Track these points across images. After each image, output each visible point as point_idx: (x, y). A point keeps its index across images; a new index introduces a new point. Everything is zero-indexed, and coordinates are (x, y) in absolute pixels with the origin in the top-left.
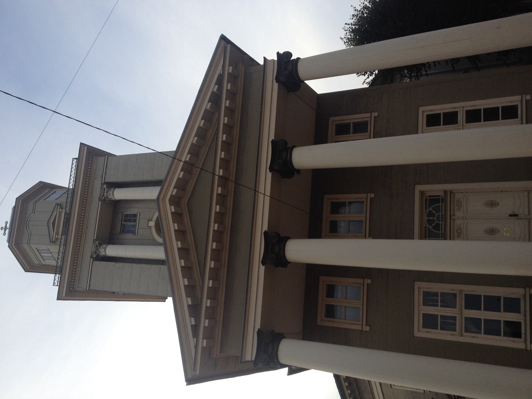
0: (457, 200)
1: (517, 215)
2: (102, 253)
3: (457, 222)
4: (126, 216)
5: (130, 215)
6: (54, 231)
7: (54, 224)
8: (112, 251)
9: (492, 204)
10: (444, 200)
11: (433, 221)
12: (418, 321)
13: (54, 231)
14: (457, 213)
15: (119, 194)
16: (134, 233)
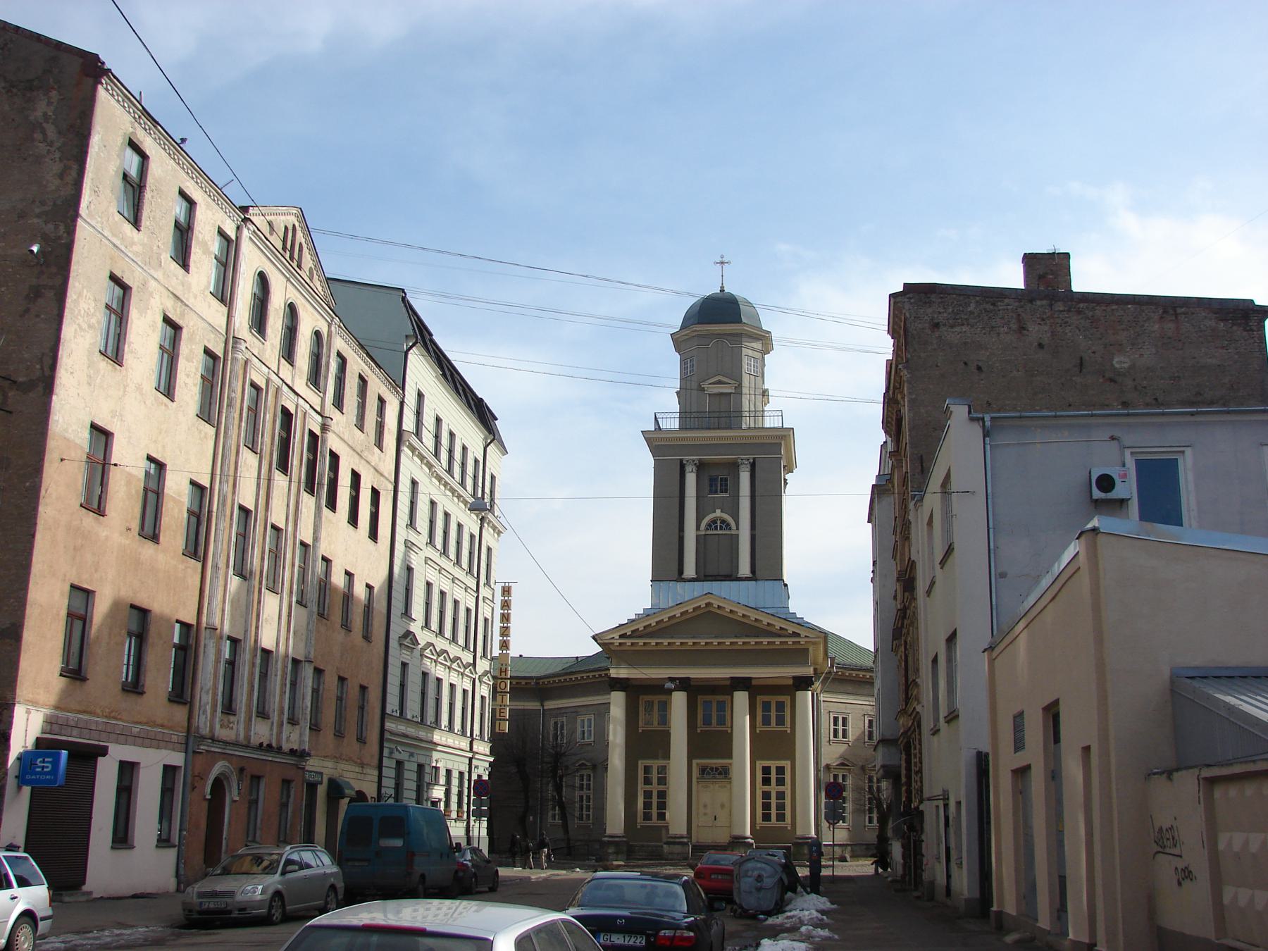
0: (728, 786)
1: (715, 819)
2: (688, 468)
3: (712, 786)
4: (726, 480)
5: (726, 485)
6: (710, 384)
7: (720, 382)
8: (691, 479)
9: (723, 806)
10: (726, 777)
11: (712, 771)
12: (648, 762)
13: (710, 384)
14: (717, 785)
15: (745, 477)
16: (711, 492)
